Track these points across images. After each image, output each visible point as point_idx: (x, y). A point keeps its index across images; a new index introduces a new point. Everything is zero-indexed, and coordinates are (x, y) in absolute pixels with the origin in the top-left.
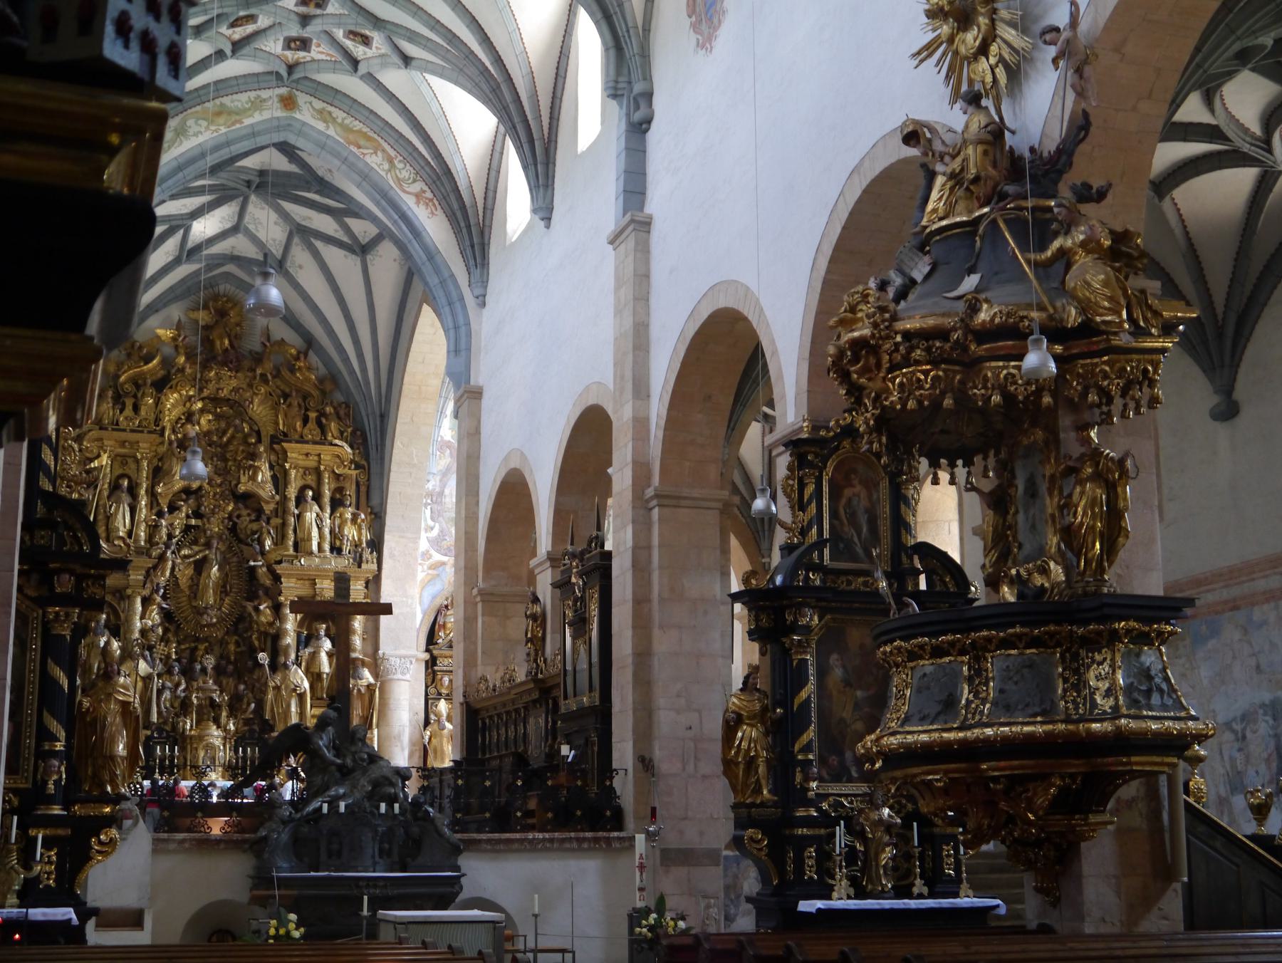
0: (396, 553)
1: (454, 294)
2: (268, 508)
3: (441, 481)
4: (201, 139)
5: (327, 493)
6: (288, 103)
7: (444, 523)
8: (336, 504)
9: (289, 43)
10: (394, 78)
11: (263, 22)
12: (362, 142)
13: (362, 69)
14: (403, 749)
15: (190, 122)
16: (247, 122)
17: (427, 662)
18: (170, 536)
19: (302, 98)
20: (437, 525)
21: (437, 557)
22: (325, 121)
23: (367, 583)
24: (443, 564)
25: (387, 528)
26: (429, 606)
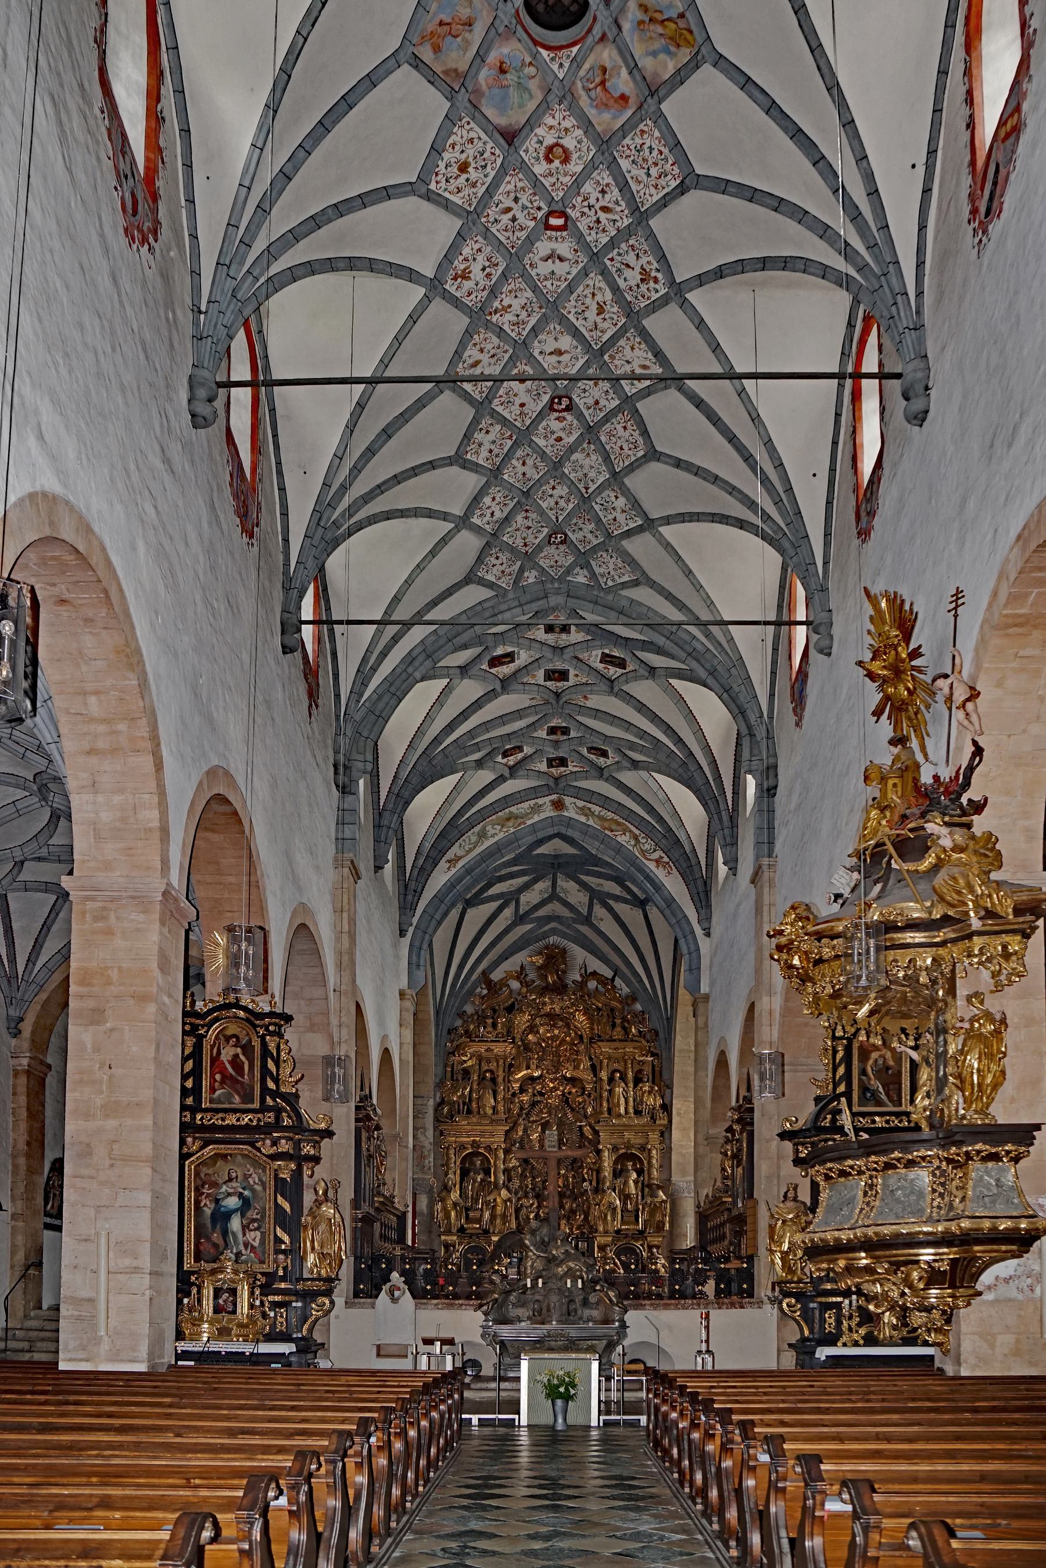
1: (687, 930)
2: (589, 1087)
4: (496, 838)
5: (630, 1075)
6: (558, 805)
8: (637, 1081)
9: (550, 763)
10: (628, 777)
11: (527, 750)
12: (614, 827)
13: (606, 774)
15: (489, 828)
16: (529, 822)
18: (522, 1109)
19: (568, 801)
22: (586, 815)
23: (662, 1134)
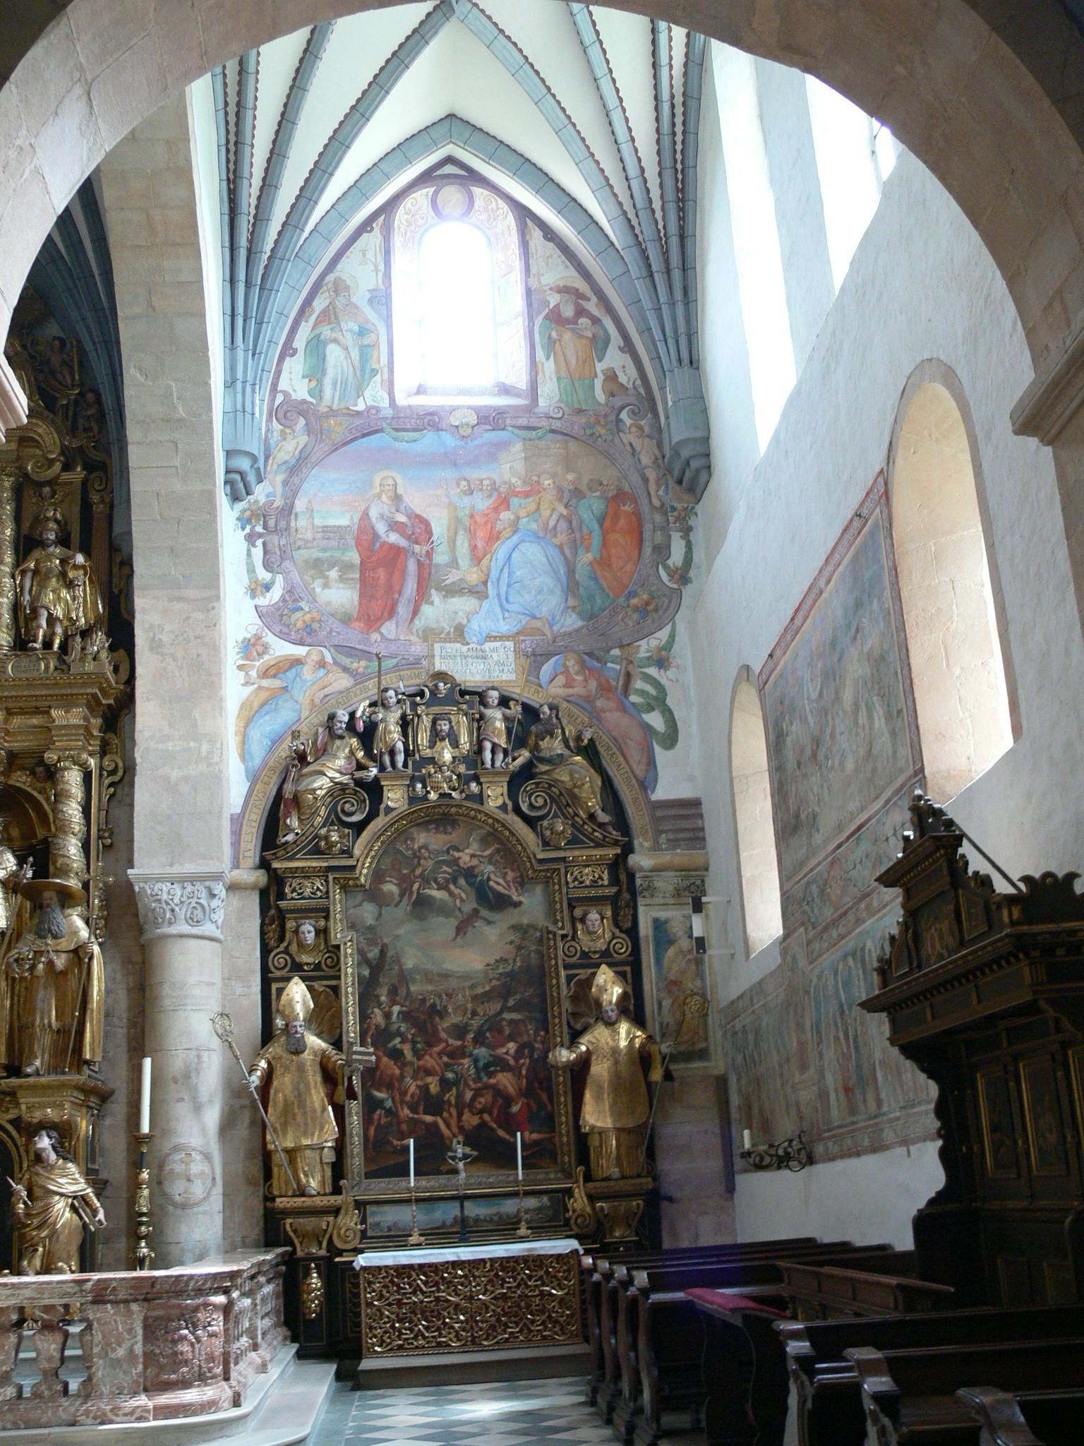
0: (165, 638)
3: (285, 483)
7: (295, 575)
14: (198, 1108)
17: (264, 893)
20: (279, 579)
21: (282, 649)
24: (297, 662)
25: (137, 581)
26: (265, 763)
